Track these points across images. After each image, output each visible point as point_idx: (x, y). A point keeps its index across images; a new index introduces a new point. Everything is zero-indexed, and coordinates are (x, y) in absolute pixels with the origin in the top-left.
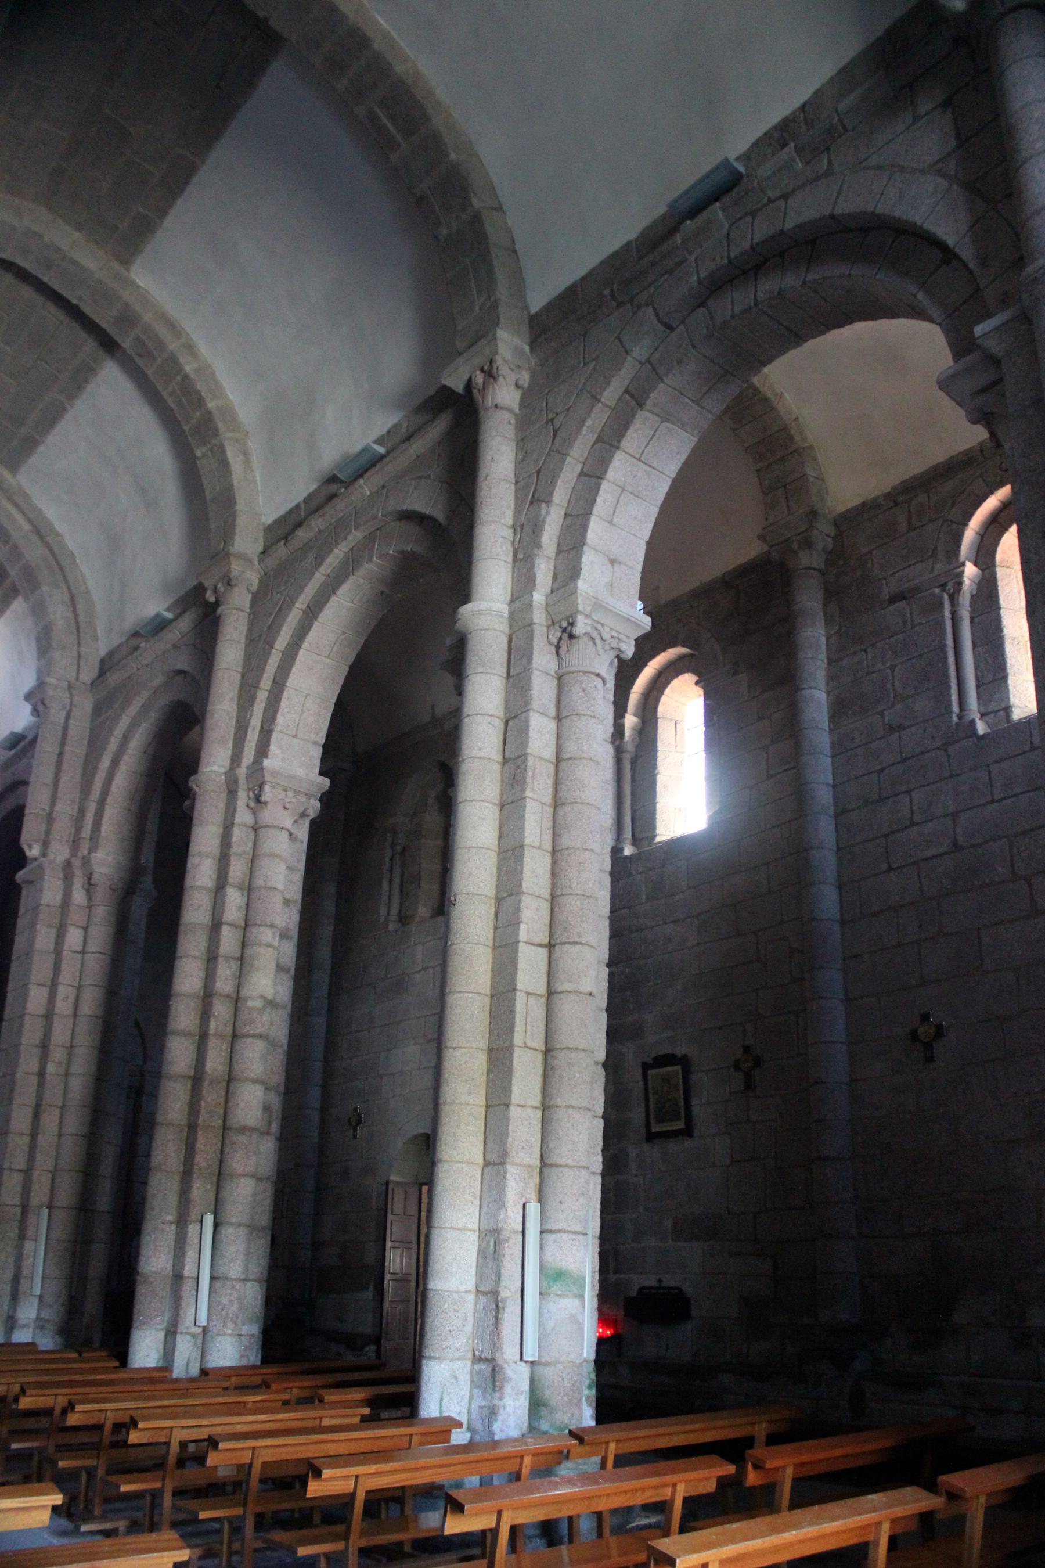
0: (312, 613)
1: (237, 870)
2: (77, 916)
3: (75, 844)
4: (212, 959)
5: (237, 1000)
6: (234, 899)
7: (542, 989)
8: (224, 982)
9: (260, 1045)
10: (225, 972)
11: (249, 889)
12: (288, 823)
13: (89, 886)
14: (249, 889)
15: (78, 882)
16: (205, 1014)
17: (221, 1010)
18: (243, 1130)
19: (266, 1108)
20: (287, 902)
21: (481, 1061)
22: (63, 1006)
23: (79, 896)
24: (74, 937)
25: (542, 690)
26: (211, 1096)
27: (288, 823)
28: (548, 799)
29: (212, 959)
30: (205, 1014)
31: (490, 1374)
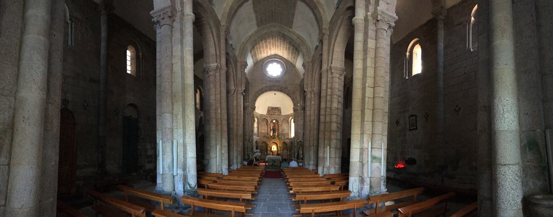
0: (337, 36)
1: (329, 85)
2: (313, 99)
3: (311, 87)
4: (326, 101)
5: (331, 108)
6: (329, 90)
7: (372, 97)
8: (328, 106)
9: (335, 116)
10: (328, 103)
11: (331, 88)
12: (338, 76)
13: (314, 94)
14: (331, 88)
15: (313, 94)
16: (326, 111)
17: (328, 110)
18: (333, 131)
19: (338, 127)
20: (339, 91)
21: (360, 112)
22: (312, 114)
23: (313, 96)
24: (313, 102)
25: (371, 33)
26: (327, 125)
27: (338, 76)
28: (373, 56)
29: (326, 101)
30: (326, 111)
31: (362, 181)
